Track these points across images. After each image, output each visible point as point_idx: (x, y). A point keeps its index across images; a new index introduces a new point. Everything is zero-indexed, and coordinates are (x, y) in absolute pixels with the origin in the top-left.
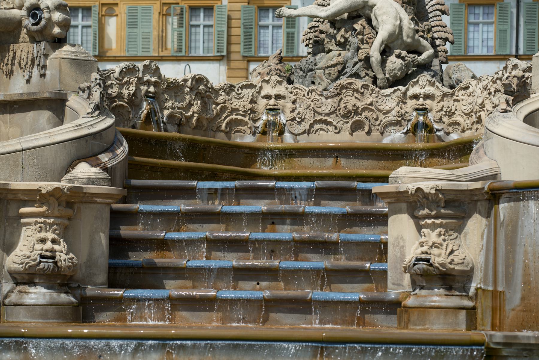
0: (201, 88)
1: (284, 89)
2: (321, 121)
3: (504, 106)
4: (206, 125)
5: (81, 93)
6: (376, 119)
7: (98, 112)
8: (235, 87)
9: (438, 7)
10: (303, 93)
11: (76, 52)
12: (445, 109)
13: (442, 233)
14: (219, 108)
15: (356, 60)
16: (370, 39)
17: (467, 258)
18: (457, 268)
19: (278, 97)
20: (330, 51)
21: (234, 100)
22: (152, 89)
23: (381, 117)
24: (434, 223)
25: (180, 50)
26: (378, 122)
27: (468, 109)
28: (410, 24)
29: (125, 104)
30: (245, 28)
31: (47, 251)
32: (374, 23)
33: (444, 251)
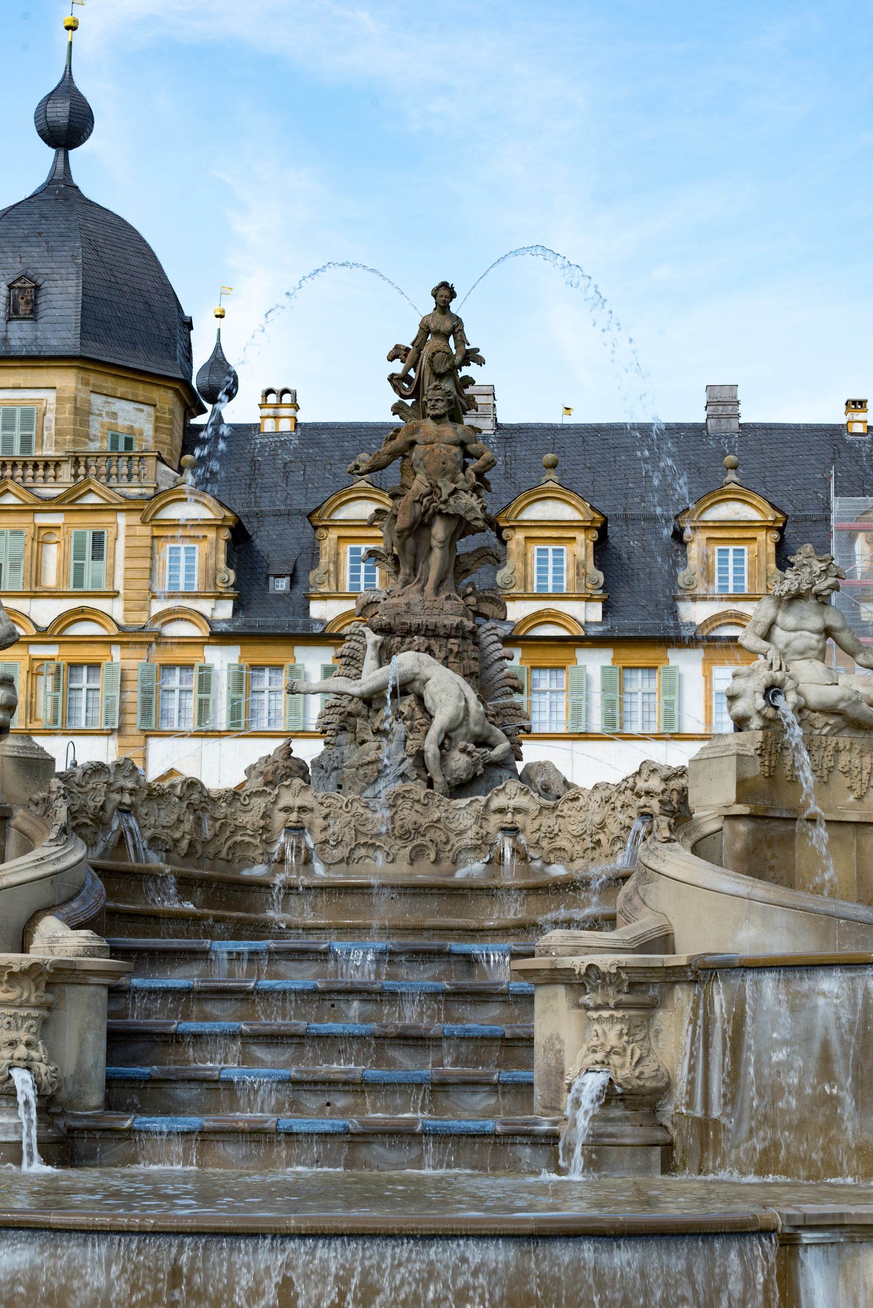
0: (194, 797)
1: (311, 799)
2: (365, 844)
3: (667, 834)
4: (200, 851)
5: (33, 808)
6: (446, 843)
7: (65, 837)
8: (240, 795)
9: (510, 681)
10: (339, 805)
11: (25, 747)
12: (543, 829)
13: (625, 1031)
14: (218, 824)
15: (401, 755)
16: (422, 725)
17: (662, 1069)
18: (649, 1084)
19: (302, 809)
20: (363, 742)
21: (239, 814)
22: (127, 799)
23: (454, 839)
24: (612, 1016)
25: (55, 721)
26: (449, 847)
27: (577, 829)
28: (478, 706)
29: (90, 822)
30: (143, 691)
31: (19, 1059)
32: (428, 703)
33: (628, 1059)
